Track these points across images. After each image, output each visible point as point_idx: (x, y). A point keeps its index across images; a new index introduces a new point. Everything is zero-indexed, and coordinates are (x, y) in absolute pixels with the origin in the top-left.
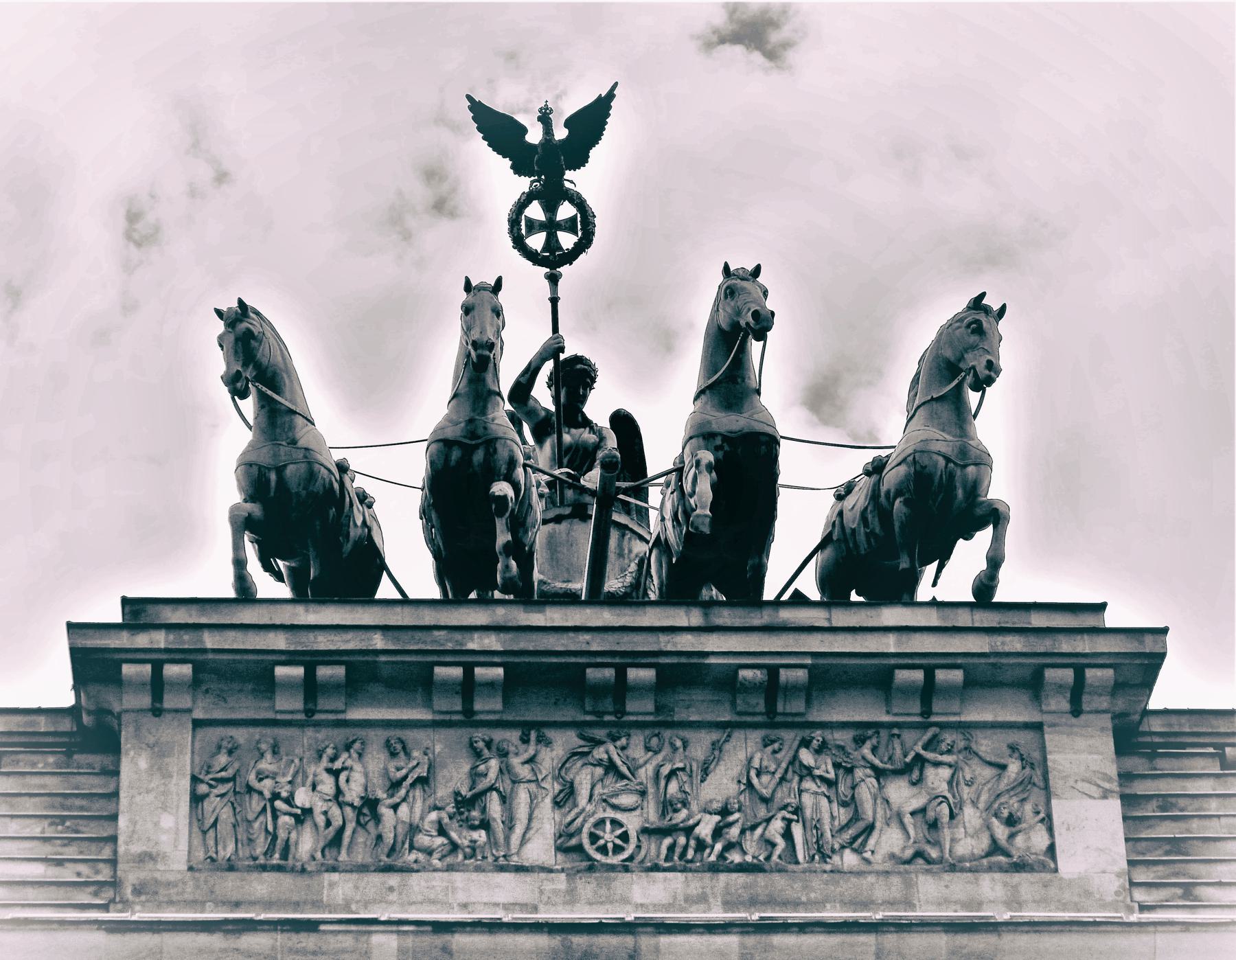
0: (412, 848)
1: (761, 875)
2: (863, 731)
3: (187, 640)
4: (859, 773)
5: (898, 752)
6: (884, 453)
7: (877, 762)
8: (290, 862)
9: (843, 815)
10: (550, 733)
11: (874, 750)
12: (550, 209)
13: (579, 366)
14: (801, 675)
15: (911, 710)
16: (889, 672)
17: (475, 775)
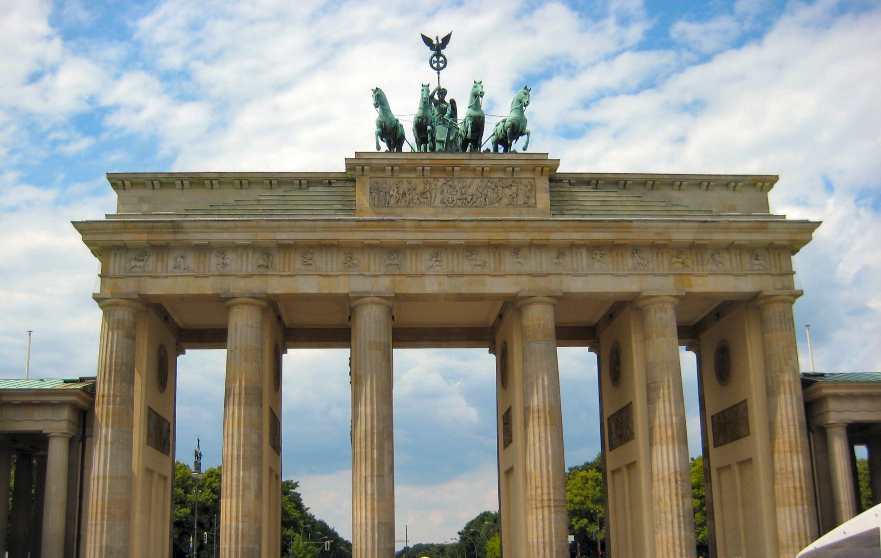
0: (413, 202)
2: (500, 179)
3: (368, 162)
4: (499, 188)
5: (507, 184)
6: (505, 118)
7: (503, 186)
8: (389, 206)
9: (496, 196)
10: (439, 179)
11: (502, 183)
12: (438, 58)
13: (443, 91)
14: (488, 169)
15: (510, 176)
16: (506, 168)
17: (425, 188)
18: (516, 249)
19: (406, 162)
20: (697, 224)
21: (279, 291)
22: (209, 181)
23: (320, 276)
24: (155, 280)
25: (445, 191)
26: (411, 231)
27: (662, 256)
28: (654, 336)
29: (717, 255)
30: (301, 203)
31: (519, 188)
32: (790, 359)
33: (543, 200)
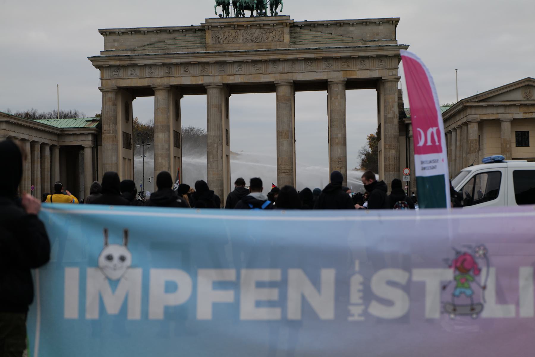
1: (259, 43)
10: (242, 30)
14: (262, 25)
17: (235, 34)
18: (274, 61)
19: (226, 24)
20: (352, 49)
21: (175, 84)
22: (143, 32)
23: (191, 77)
24: (123, 80)
25: (244, 36)
26: (228, 57)
27: (338, 63)
28: (333, 99)
29: (362, 61)
30: (183, 43)
31: (277, 33)
32: (393, 108)
33: (287, 38)
